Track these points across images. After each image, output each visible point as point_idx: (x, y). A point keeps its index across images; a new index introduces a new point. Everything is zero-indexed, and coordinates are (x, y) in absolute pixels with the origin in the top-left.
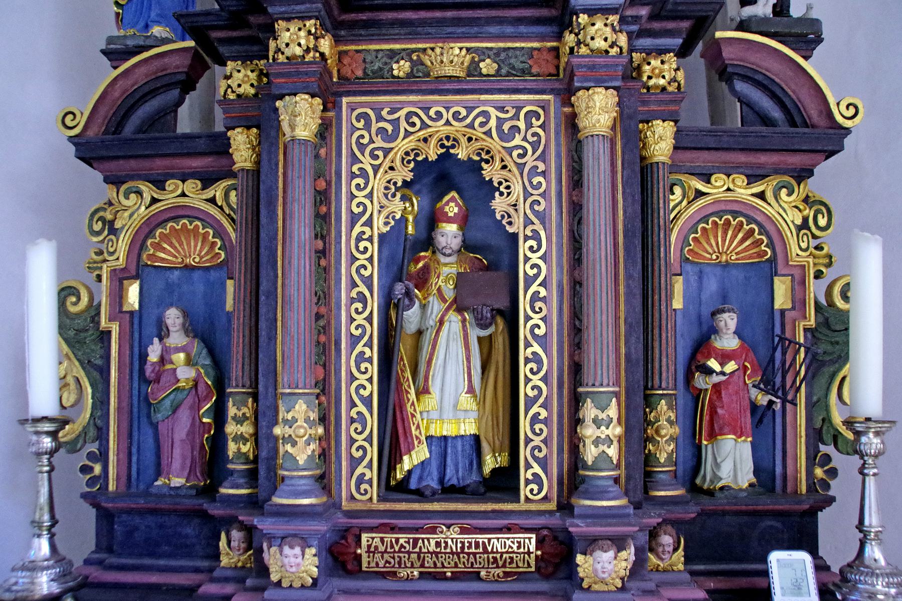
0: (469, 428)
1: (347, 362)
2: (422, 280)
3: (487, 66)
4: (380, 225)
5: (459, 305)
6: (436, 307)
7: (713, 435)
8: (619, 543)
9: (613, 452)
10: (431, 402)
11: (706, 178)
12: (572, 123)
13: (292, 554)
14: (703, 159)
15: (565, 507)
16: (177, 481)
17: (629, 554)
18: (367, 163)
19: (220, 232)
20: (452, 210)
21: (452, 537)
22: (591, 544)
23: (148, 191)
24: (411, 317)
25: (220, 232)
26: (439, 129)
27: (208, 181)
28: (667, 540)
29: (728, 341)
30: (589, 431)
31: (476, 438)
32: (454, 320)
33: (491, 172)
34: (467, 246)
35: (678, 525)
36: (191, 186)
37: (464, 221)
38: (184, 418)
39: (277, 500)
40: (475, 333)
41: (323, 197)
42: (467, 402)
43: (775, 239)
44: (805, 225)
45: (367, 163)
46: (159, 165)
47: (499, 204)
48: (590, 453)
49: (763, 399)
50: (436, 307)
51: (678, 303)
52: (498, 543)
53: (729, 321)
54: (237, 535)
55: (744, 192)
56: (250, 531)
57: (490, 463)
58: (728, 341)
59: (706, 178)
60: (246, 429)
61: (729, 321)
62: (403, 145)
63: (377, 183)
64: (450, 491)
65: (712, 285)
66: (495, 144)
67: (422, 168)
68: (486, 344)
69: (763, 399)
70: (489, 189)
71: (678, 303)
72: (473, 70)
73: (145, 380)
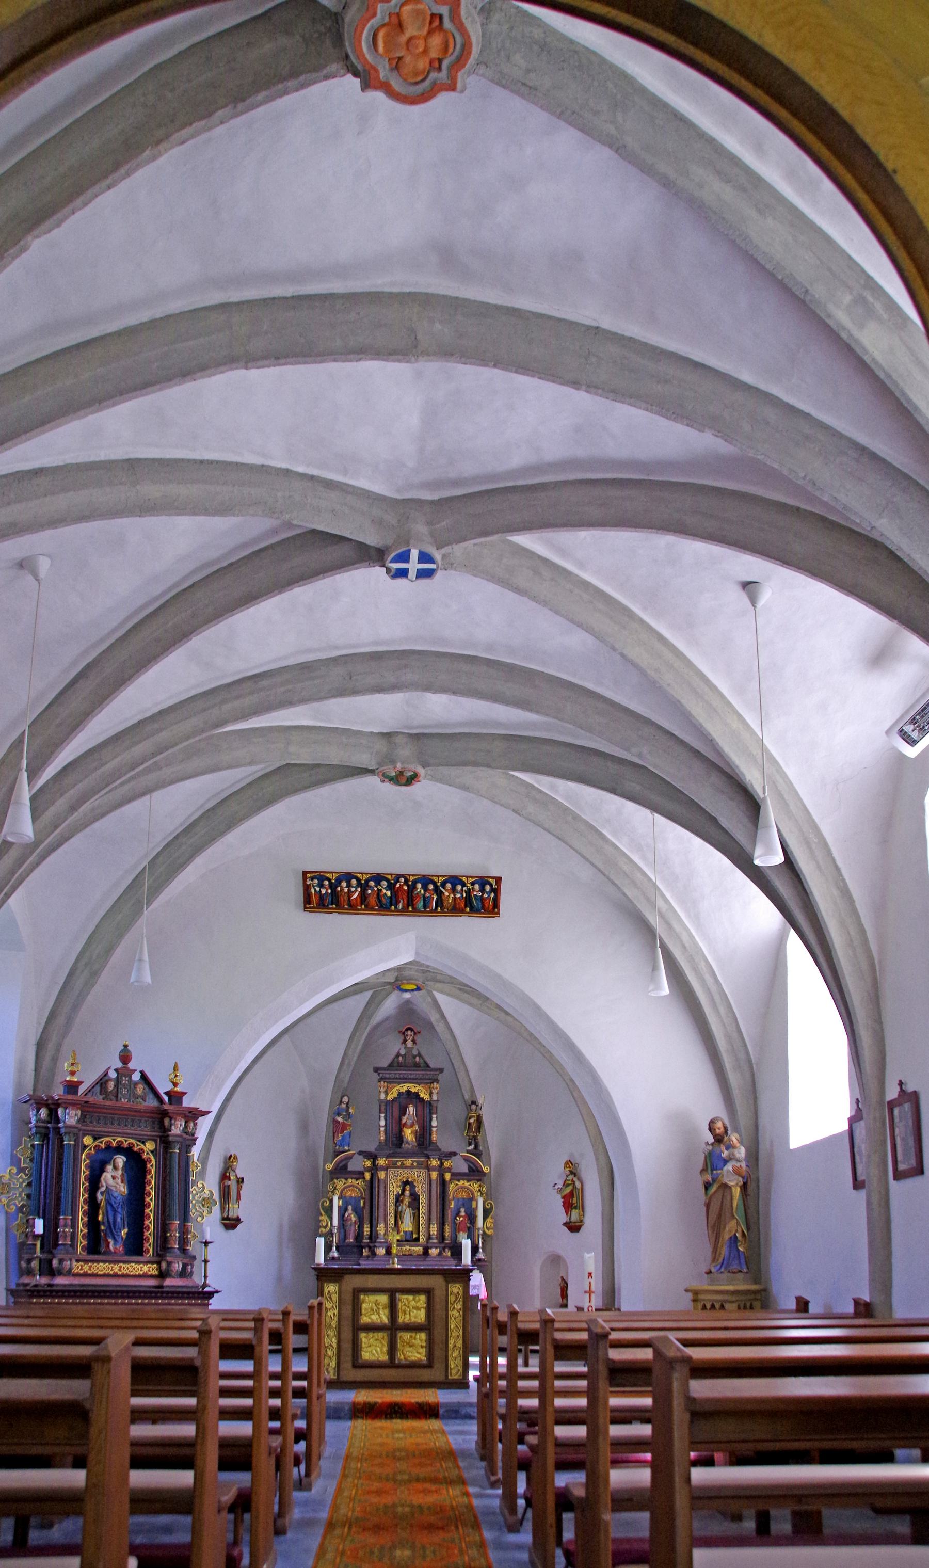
0: (411, 1229)
1: (389, 1217)
2: (402, 1202)
3: (415, 1164)
4: (395, 1193)
5: (409, 1207)
6: (404, 1207)
7: (459, 1232)
8: (436, 1248)
9: (435, 1233)
10: (404, 1224)
11: (459, 1181)
12: (430, 1175)
13: (381, 1249)
14: (459, 1177)
15: (427, 1242)
16: (351, 1240)
17: (438, 1250)
18: (393, 1181)
19: (359, 1190)
20: (408, 1189)
21: (408, 1248)
22: (431, 1248)
23: (344, 1181)
24: (400, 1208)
25: (359, 1190)
26: (406, 1175)
27: (357, 1179)
28: (447, 1250)
29: (463, 1214)
30: (431, 1229)
31: (412, 1232)
32: (408, 1210)
33: (415, 1183)
34: (411, 1195)
35: (450, 1248)
36: (354, 1181)
37: (410, 1191)
38: (353, 1228)
39: (378, 1240)
40: (412, 1212)
41: (385, 1187)
42: (410, 1224)
43: (473, 1194)
44: (480, 1190)
45: (393, 1181)
46: (347, 1176)
47: (417, 1189)
48: (431, 1233)
49: (468, 1225)
50: (404, 1207)
51: (452, 1206)
52: (416, 1249)
53: (463, 1210)
54: (367, 1249)
55: (466, 1184)
56: (370, 1247)
57: (415, 1236)
58: (463, 1214)
59: (459, 1181)
60: (369, 1229)
61: (463, 1210)
62: (399, 1178)
63: (395, 1185)
64: (407, 1241)
65: (461, 1203)
66: (416, 1178)
67: (403, 1182)
68: (414, 1214)
69: (468, 1225)
70: (415, 1187)
71: (452, 1206)
72: (412, 1164)
73: (343, 1220)
